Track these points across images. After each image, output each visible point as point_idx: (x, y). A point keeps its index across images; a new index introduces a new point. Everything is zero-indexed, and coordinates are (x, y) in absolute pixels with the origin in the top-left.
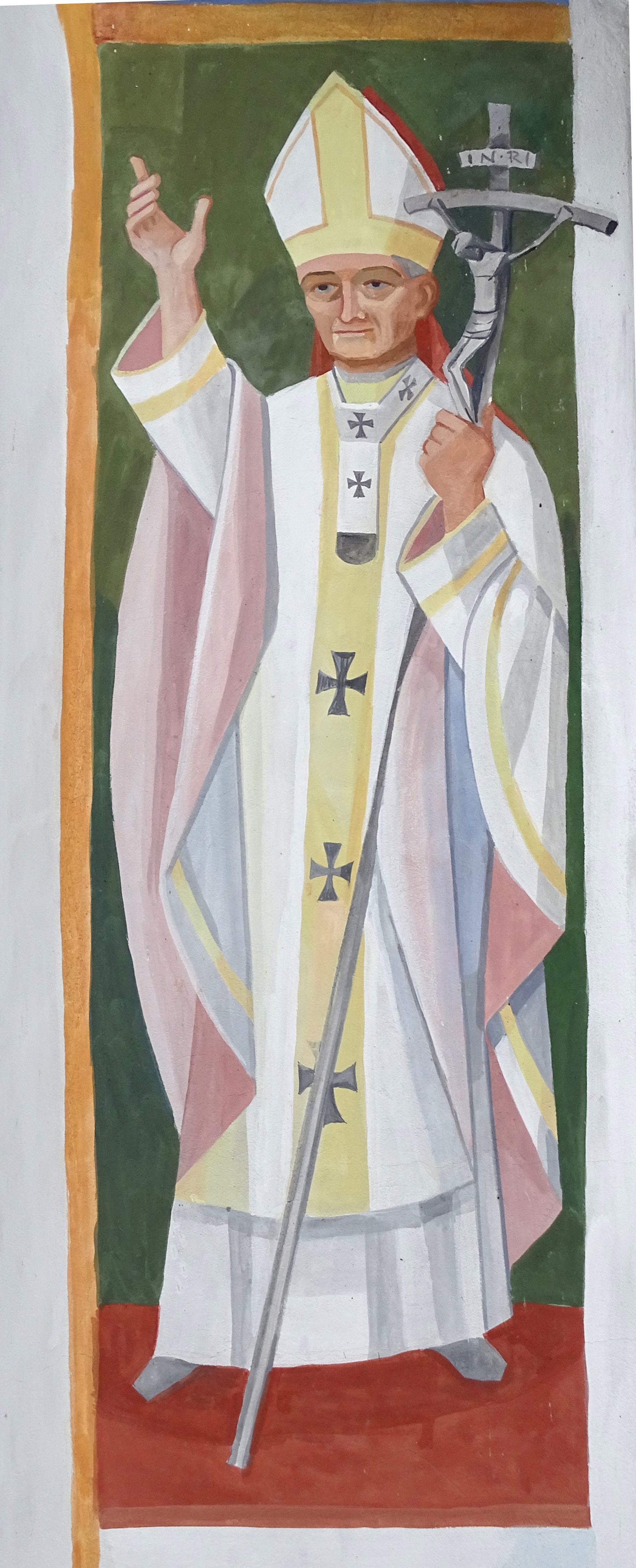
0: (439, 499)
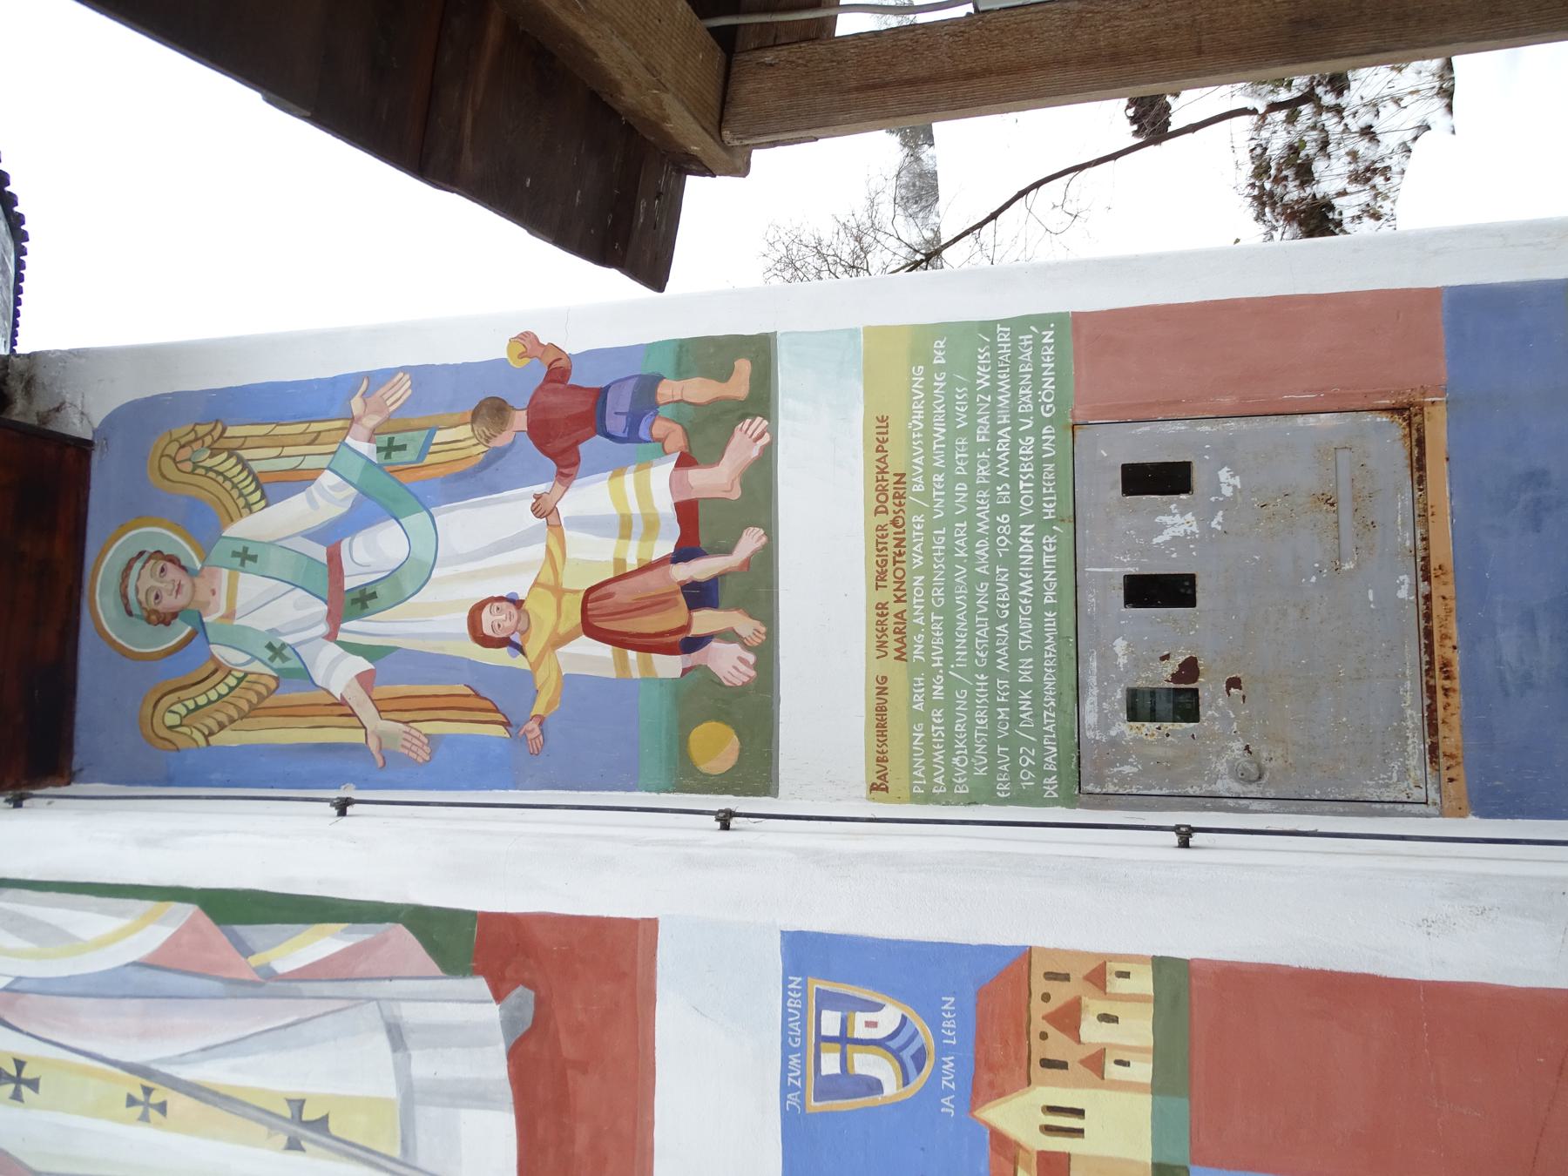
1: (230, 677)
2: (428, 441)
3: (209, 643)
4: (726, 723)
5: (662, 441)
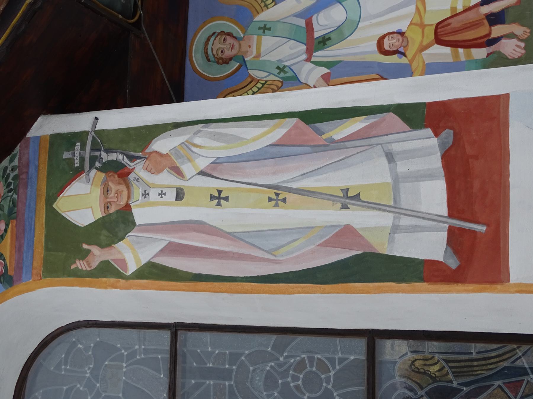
0: (167, 168)
1: (259, 84)
3: (248, 70)
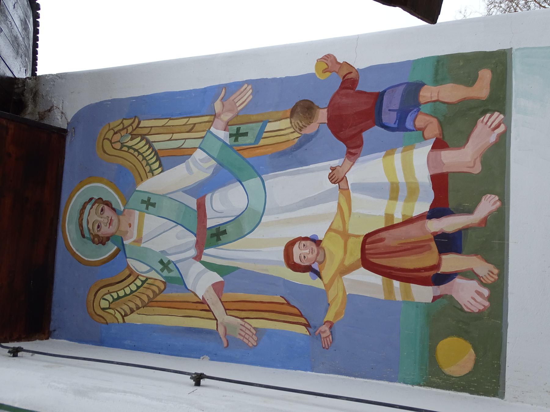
1: (138, 280)
2: (262, 131)
3: (126, 257)
4: (466, 339)
5: (422, 130)
